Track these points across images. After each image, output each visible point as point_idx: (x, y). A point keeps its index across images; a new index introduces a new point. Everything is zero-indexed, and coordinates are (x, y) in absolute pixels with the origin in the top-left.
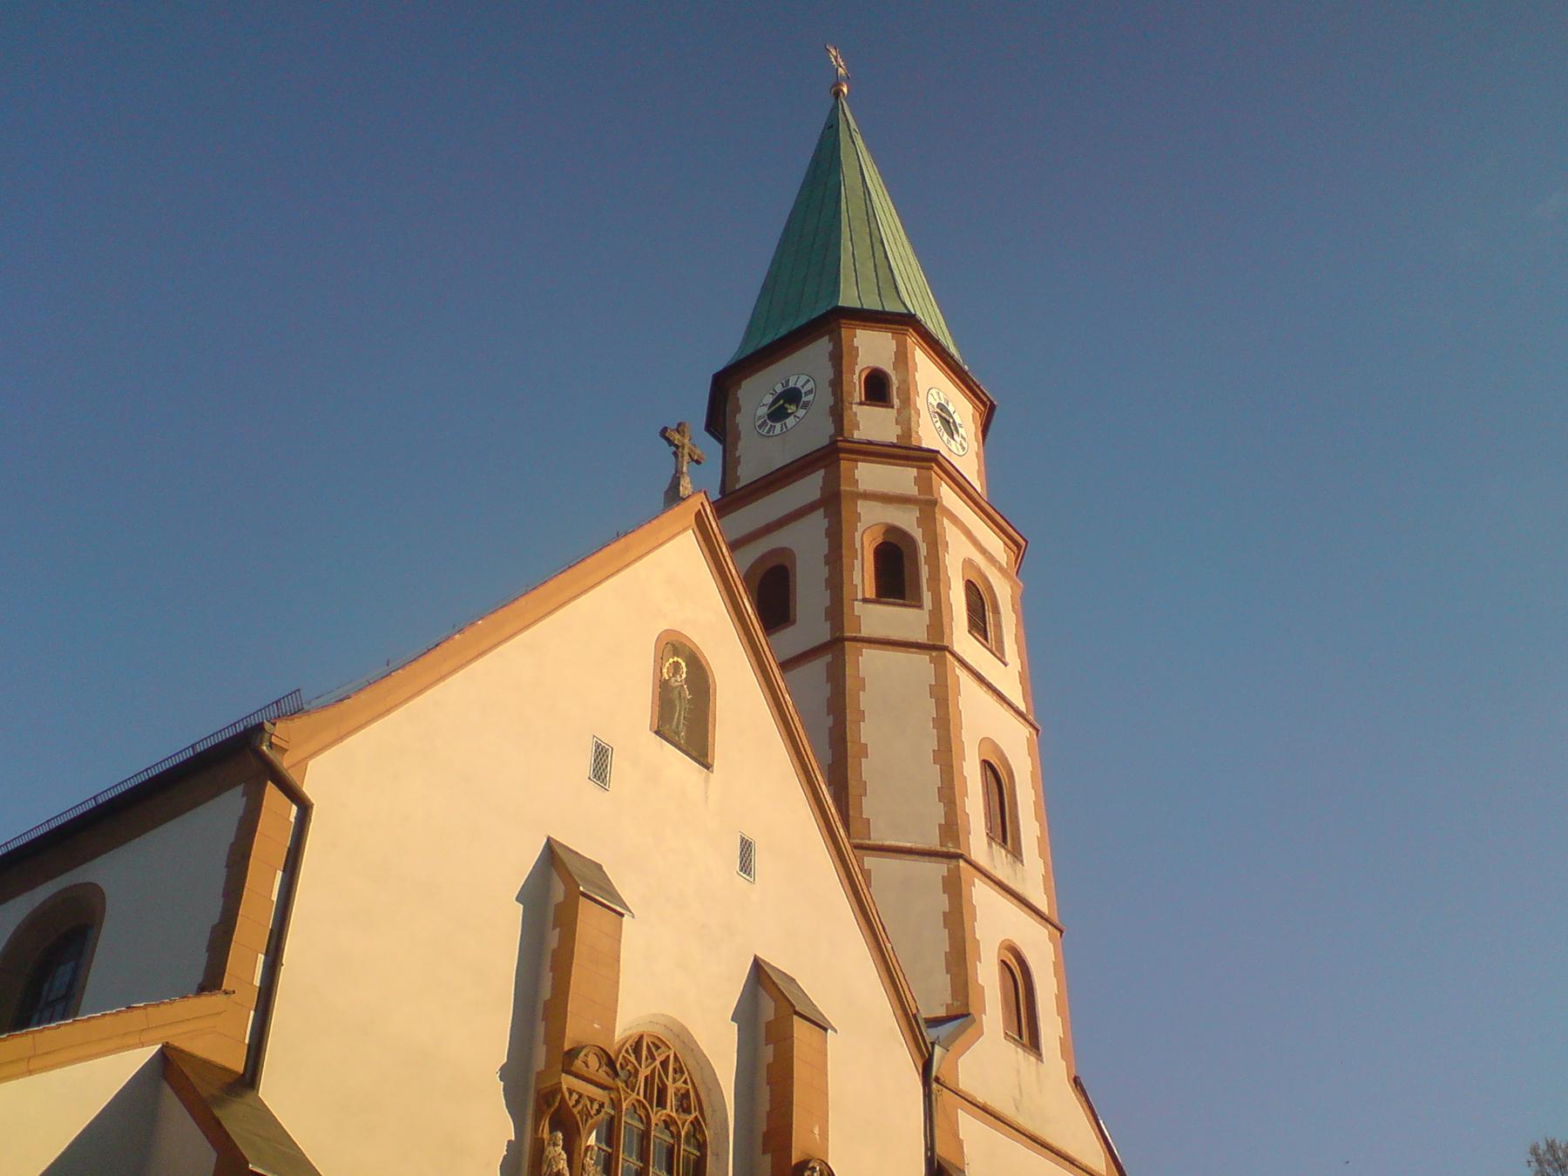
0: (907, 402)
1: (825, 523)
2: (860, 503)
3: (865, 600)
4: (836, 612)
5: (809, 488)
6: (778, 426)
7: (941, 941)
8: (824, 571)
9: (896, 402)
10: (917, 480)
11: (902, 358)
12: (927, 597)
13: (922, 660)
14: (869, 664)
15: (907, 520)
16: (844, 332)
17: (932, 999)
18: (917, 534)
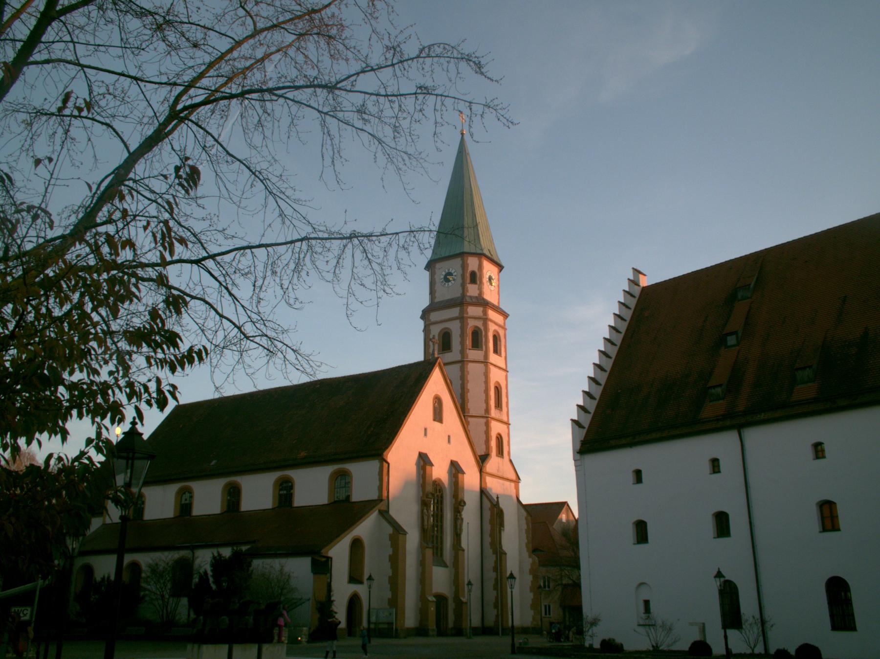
0: (481, 282)
1: (460, 325)
2: (469, 319)
3: (470, 349)
4: (463, 352)
5: (455, 312)
6: (447, 284)
7: (484, 437)
8: (459, 339)
9: (478, 282)
10: (483, 311)
11: (480, 267)
12: (484, 347)
13: (482, 365)
14: (471, 367)
15: (479, 324)
16: (465, 259)
17: (481, 451)
18: (482, 328)
